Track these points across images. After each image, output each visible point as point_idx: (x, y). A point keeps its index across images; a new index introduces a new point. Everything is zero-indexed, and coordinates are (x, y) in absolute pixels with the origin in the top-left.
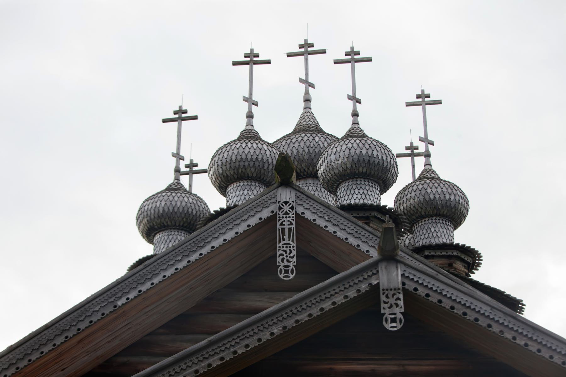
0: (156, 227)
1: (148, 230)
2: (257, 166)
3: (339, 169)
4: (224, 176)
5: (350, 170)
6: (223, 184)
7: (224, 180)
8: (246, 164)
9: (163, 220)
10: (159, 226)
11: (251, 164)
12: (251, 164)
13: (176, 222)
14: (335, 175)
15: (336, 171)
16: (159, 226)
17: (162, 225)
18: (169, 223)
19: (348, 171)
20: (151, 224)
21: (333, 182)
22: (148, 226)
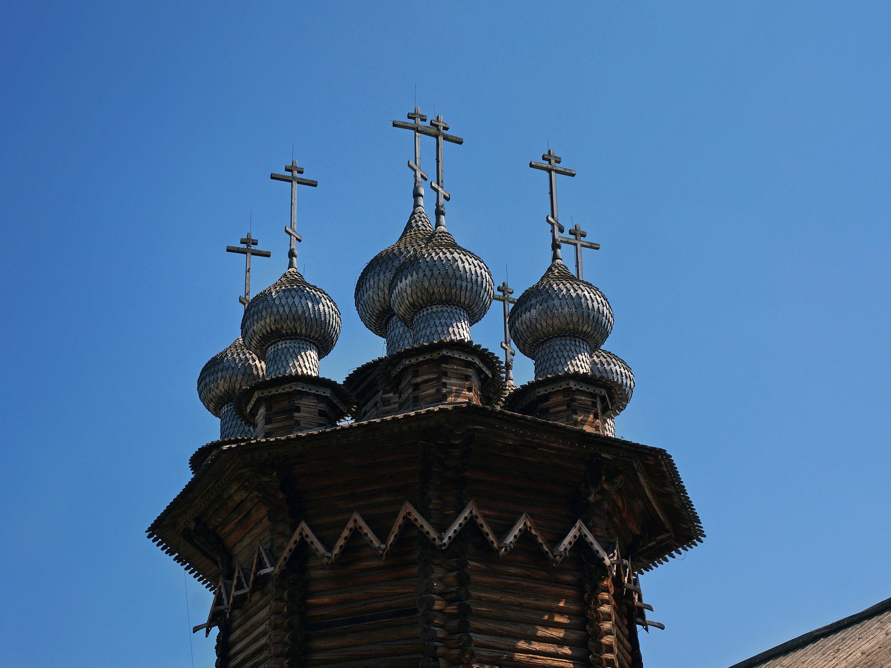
1: (270, 334)
3: (561, 319)
5: (574, 325)
9: (297, 325)
10: (289, 332)
13: (312, 332)
14: (553, 327)
16: (289, 332)
17: (294, 331)
18: (304, 331)
19: (571, 326)
21: (542, 334)
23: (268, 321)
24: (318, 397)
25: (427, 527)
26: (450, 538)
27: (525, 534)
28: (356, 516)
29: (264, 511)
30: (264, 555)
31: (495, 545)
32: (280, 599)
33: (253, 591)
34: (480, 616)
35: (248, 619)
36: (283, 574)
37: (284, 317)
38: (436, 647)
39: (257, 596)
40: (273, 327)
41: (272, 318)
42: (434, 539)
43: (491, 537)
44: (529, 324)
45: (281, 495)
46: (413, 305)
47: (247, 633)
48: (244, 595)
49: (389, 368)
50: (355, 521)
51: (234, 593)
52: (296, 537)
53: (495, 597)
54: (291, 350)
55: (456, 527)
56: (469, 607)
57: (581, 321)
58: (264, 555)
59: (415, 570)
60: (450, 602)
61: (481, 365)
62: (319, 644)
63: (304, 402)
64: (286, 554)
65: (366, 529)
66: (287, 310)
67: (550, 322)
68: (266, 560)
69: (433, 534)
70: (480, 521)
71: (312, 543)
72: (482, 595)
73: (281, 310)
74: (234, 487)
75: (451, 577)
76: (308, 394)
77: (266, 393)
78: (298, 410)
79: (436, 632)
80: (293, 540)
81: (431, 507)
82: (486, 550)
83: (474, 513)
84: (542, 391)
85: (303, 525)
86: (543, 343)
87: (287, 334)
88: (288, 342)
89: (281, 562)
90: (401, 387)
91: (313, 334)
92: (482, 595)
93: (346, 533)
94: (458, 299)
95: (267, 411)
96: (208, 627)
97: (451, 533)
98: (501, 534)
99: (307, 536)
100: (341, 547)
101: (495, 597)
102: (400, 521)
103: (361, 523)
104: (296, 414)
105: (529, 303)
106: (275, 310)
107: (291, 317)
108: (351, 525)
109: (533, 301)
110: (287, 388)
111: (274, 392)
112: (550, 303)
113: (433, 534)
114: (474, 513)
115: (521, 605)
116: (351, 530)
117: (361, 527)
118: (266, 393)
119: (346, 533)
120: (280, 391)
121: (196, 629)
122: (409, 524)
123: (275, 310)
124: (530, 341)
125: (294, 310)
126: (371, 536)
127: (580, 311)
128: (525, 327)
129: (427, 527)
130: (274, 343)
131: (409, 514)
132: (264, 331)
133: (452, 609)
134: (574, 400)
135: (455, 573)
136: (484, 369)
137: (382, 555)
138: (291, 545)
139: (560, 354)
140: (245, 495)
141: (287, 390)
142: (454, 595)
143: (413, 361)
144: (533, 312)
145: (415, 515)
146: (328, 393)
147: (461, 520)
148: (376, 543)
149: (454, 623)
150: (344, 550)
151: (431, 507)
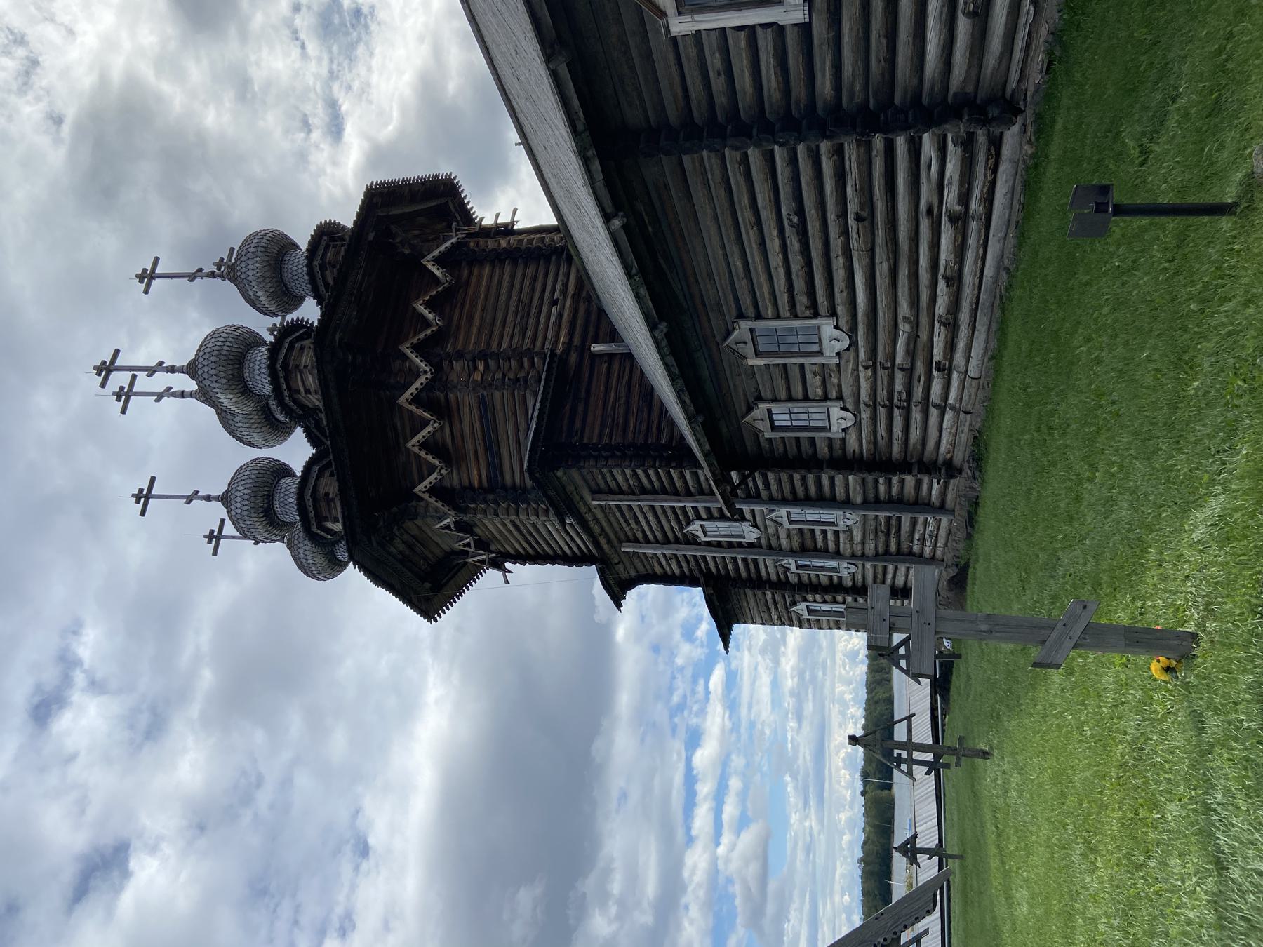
0: (266, 505)
2: (232, 340)
4: (231, 380)
6: (240, 386)
7: (237, 383)
8: (225, 348)
9: (261, 494)
10: (266, 501)
11: (228, 344)
12: (228, 344)
15: (268, 274)
16: (266, 501)
19: (272, 262)
20: (261, 509)
22: (261, 515)
23: (255, 519)
24: (318, 478)
25: (417, 385)
26: (426, 365)
27: (429, 305)
28: (409, 445)
29: (409, 524)
30: (442, 524)
31: (434, 329)
32: (475, 510)
33: (472, 533)
34: (489, 343)
35: (497, 539)
36: (458, 509)
37: (252, 505)
38: (509, 379)
39: (477, 530)
40: (261, 515)
41: (254, 515)
42: (427, 379)
43: (428, 332)
44: (270, 298)
45: (395, 509)
46: (243, 393)
47: (507, 539)
48: (475, 541)
49: (294, 415)
50: (413, 446)
51: (473, 550)
52: (426, 496)
53: (475, 331)
54: (282, 499)
55: (418, 360)
56: (480, 352)
57: (267, 254)
58: (442, 524)
59: (451, 396)
60: (476, 367)
61: (294, 336)
62: (508, 477)
63: (322, 489)
64: (439, 505)
65: (420, 437)
66: (246, 502)
67: (268, 280)
68: (445, 522)
69: (423, 379)
70: (415, 340)
71: (431, 483)
72: (472, 341)
73: (246, 508)
74: (392, 549)
75: (457, 366)
76: (315, 486)
77: (313, 521)
78: (327, 494)
79: (498, 379)
80: (429, 499)
81: (402, 382)
82: (440, 337)
83: (409, 345)
84: (322, 288)
85: (416, 490)
86: (287, 288)
87: (268, 503)
88: (275, 502)
89: (446, 509)
90: (310, 406)
91: (270, 481)
92: (472, 341)
93: (423, 454)
94: (239, 354)
95: (328, 521)
96: (505, 571)
97: (422, 364)
98: (426, 324)
99: (426, 487)
100: (433, 458)
101: (475, 331)
102: (413, 408)
103: (415, 440)
104: (331, 496)
105: (252, 297)
106: (246, 513)
107: (253, 499)
108: (416, 450)
109: (251, 293)
110: (309, 503)
111: (312, 515)
112: (251, 278)
113: (423, 379)
114: (409, 345)
115: (483, 310)
116: (420, 450)
117: (419, 441)
118: (313, 521)
119: (423, 454)
120: (311, 509)
121: (507, 582)
122: (416, 400)
123: (246, 513)
124: (285, 299)
125: (246, 497)
126: (425, 432)
127: (259, 254)
128: (273, 302)
129: (417, 385)
130: (276, 514)
131: (407, 399)
132: (266, 522)
133: (481, 366)
134: (329, 263)
135: (454, 362)
136: (297, 334)
137: (440, 424)
138: (432, 500)
139: (295, 273)
140: (399, 540)
141: (311, 504)
142: (470, 363)
143: (286, 393)
144: (259, 294)
145: (408, 394)
146: (316, 468)
147: (413, 356)
148: (429, 429)
149: (492, 363)
150: (436, 456)
151: (402, 382)
